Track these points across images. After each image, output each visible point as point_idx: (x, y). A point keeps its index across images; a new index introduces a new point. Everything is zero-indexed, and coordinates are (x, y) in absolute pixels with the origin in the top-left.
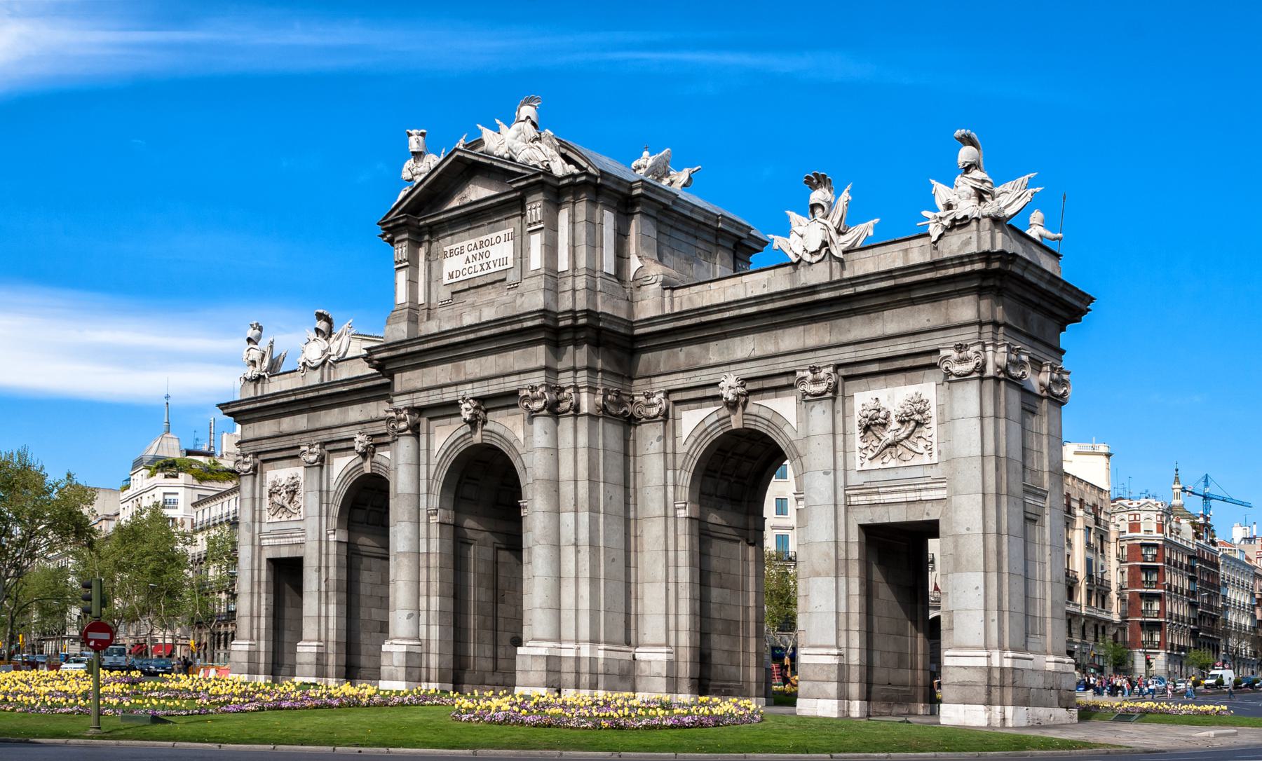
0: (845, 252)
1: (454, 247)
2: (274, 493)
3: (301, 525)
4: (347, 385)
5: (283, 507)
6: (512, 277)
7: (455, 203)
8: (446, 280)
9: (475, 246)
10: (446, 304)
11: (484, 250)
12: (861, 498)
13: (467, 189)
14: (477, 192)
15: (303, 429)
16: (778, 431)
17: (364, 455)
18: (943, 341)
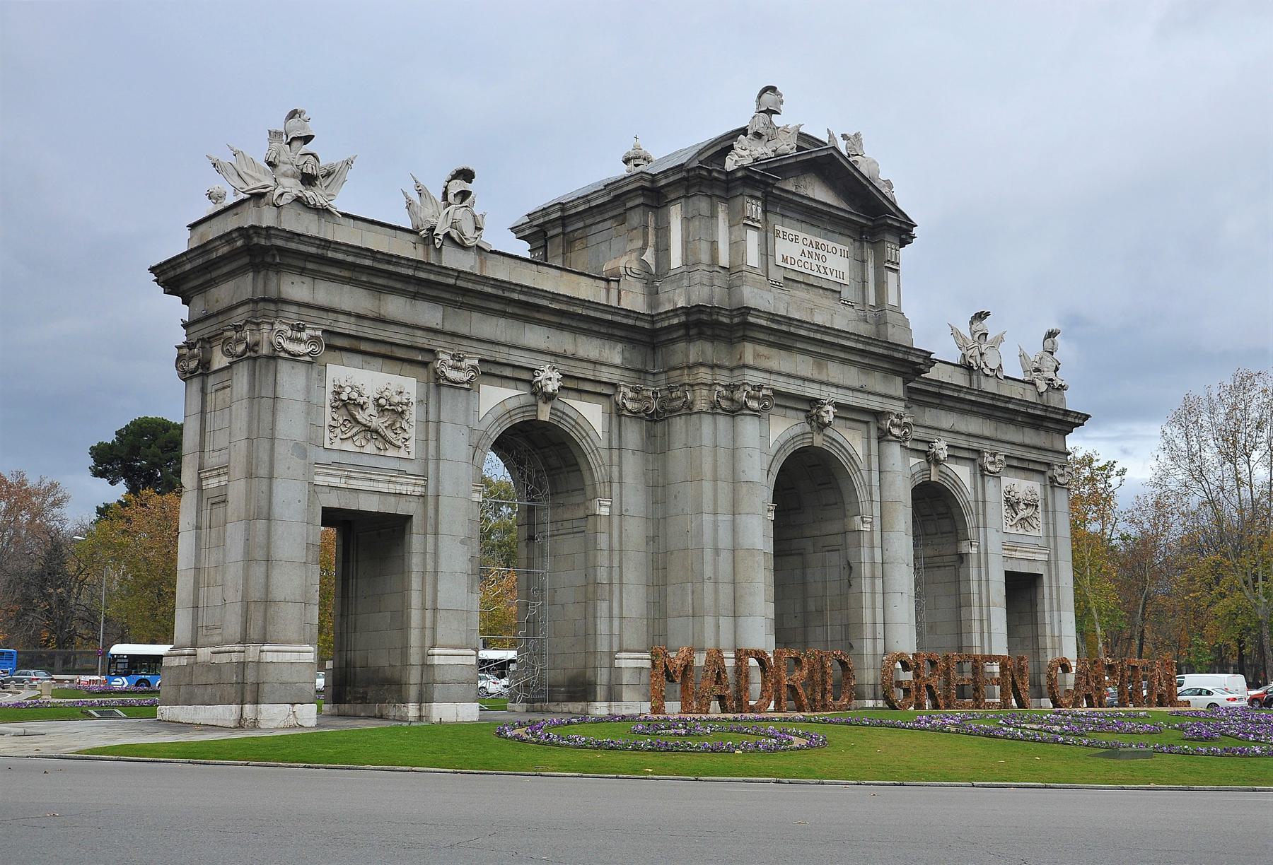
0: (1005, 377)
1: (789, 231)
2: (358, 404)
3: (409, 468)
4: (559, 301)
5: (377, 432)
6: (845, 294)
7: (790, 186)
8: (779, 261)
9: (811, 243)
10: (778, 285)
11: (822, 253)
12: (1006, 552)
13: (802, 177)
14: (819, 193)
15: (433, 325)
16: (960, 491)
17: (549, 397)
18: (1051, 459)
